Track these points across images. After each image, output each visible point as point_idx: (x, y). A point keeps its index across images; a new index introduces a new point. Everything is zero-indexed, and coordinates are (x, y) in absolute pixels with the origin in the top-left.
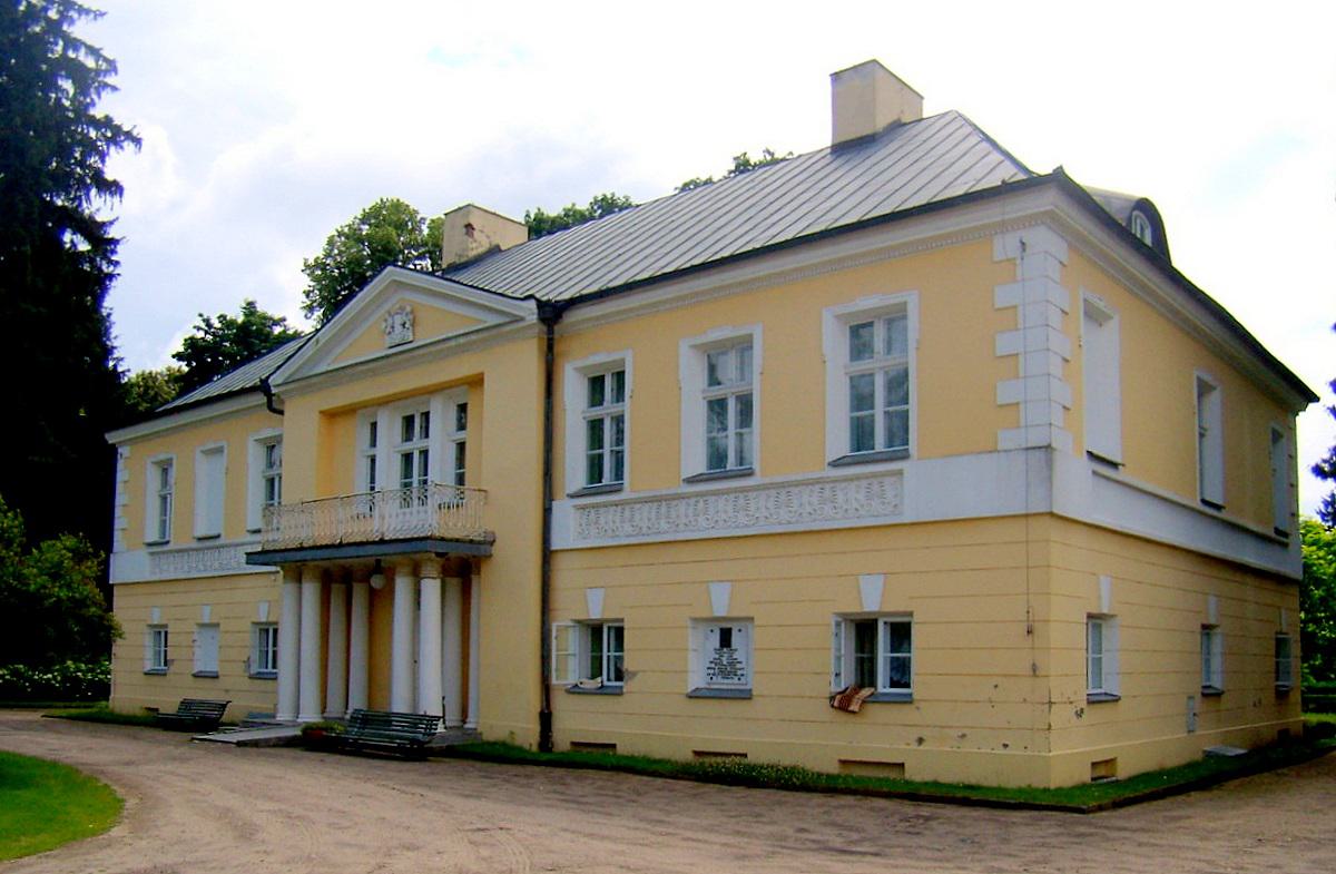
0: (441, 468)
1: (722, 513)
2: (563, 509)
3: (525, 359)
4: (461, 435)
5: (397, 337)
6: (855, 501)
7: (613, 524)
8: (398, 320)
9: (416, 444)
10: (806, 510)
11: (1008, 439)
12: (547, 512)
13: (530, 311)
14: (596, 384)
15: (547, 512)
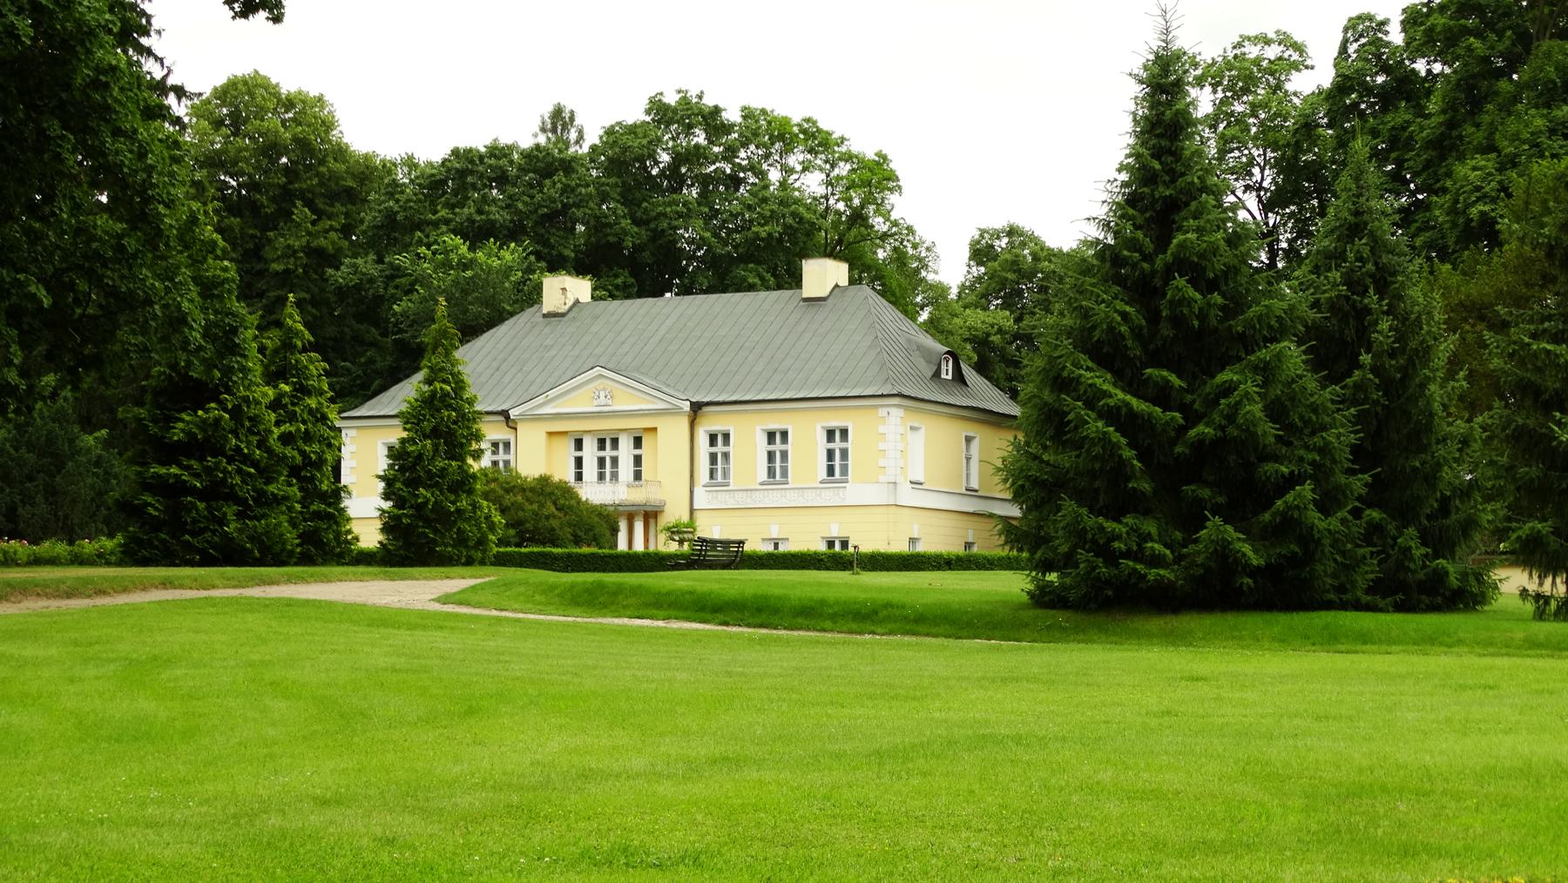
0: (626, 469)
1: (774, 497)
2: (699, 491)
3: (683, 424)
4: (638, 452)
5: (602, 400)
6: (830, 496)
7: (723, 499)
8: (602, 394)
9: (608, 453)
10: (810, 499)
11: (882, 479)
12: (692, 492)
13: (686, 406)
14: (713, 439)
15: (692, 492)
